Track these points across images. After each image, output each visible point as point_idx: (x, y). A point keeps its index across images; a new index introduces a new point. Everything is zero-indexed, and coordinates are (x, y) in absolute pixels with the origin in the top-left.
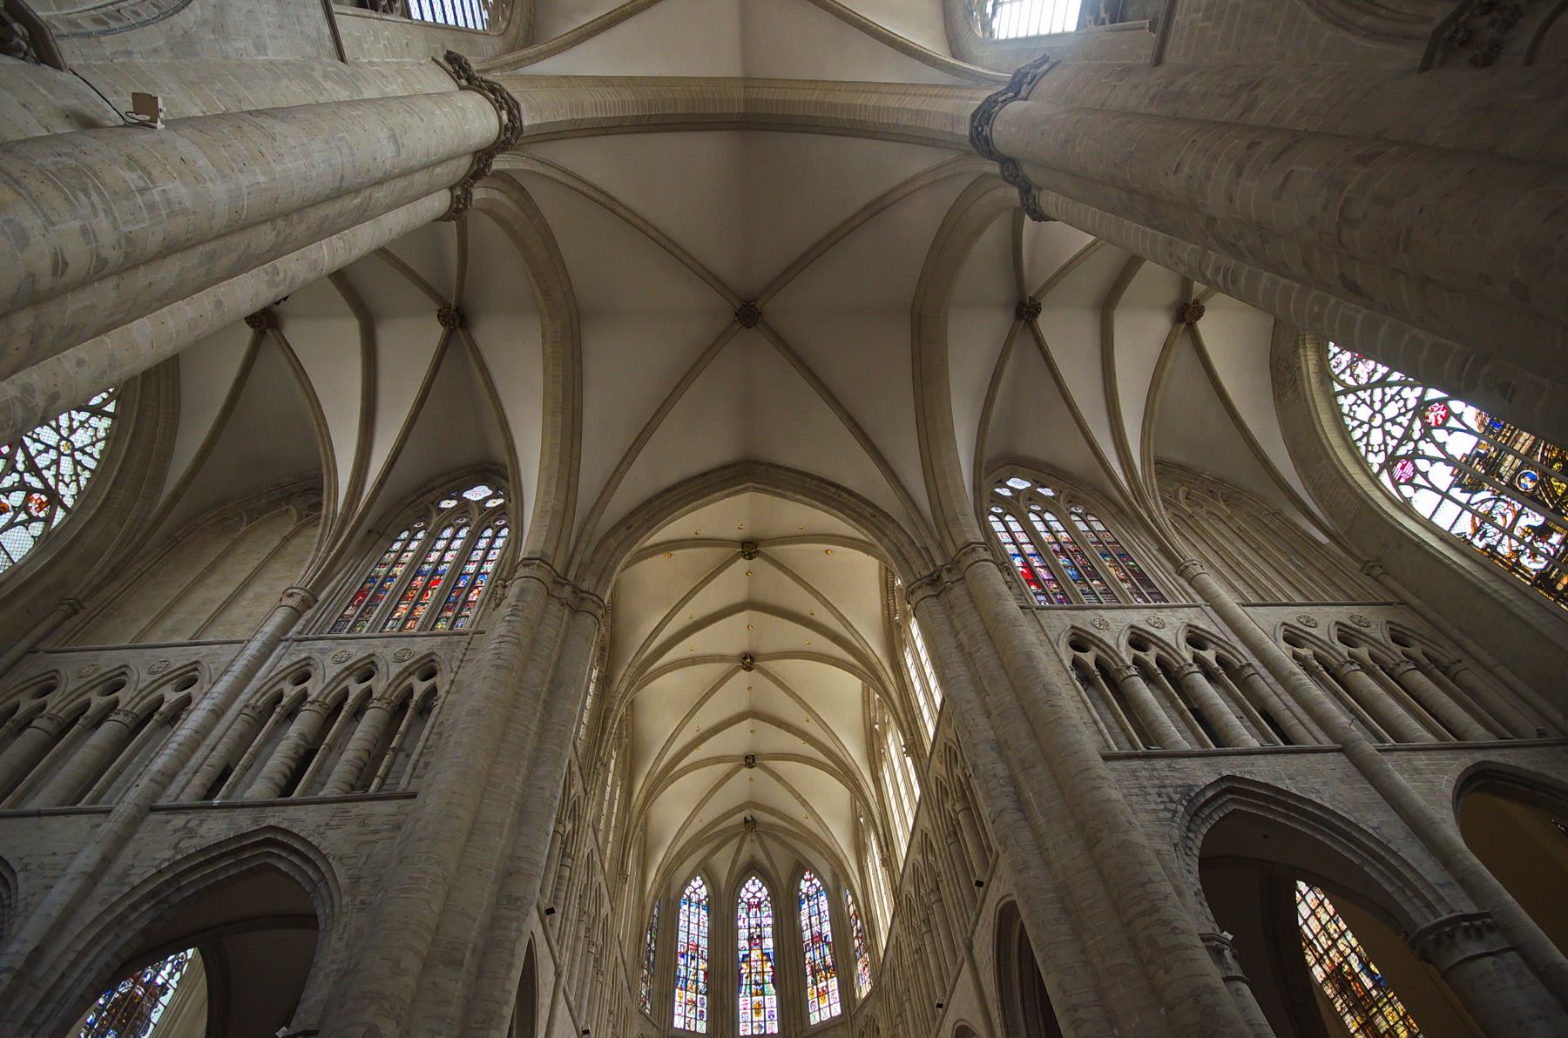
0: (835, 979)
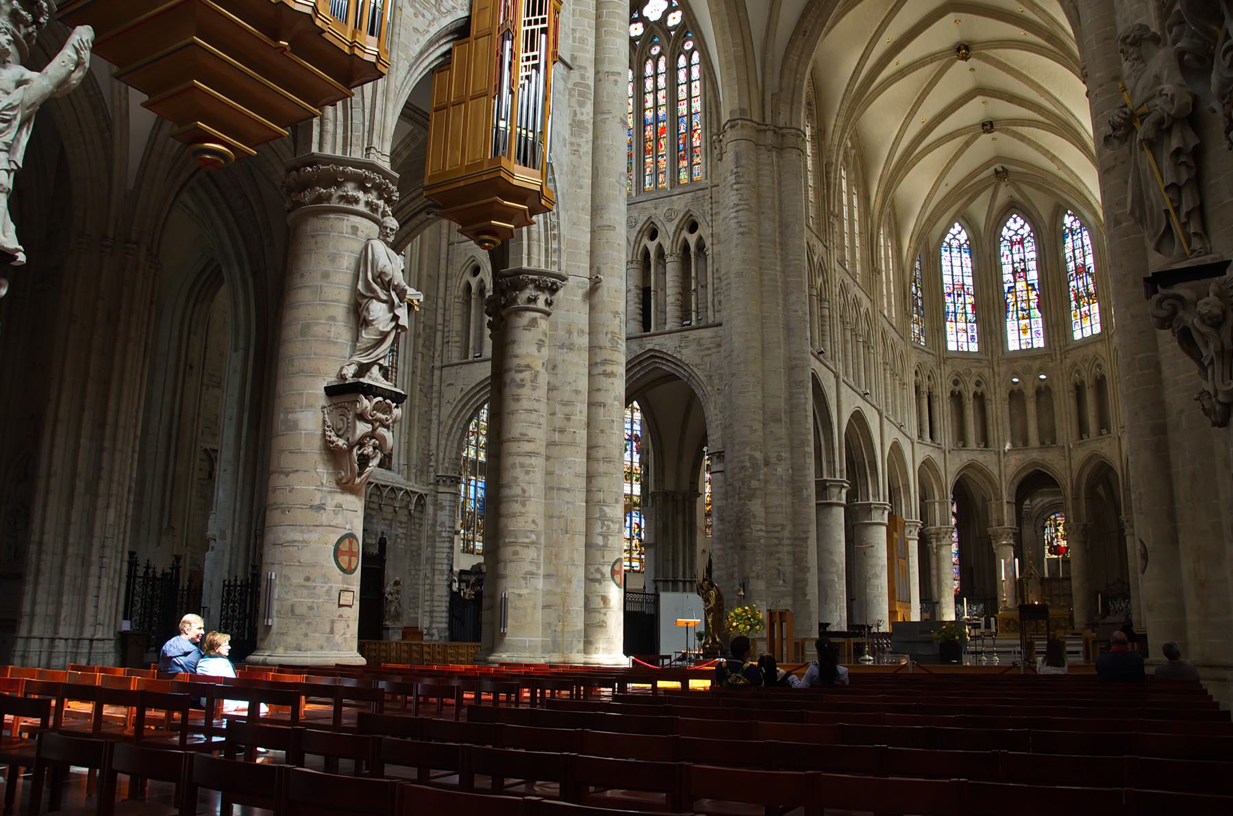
0: (1097, 304)
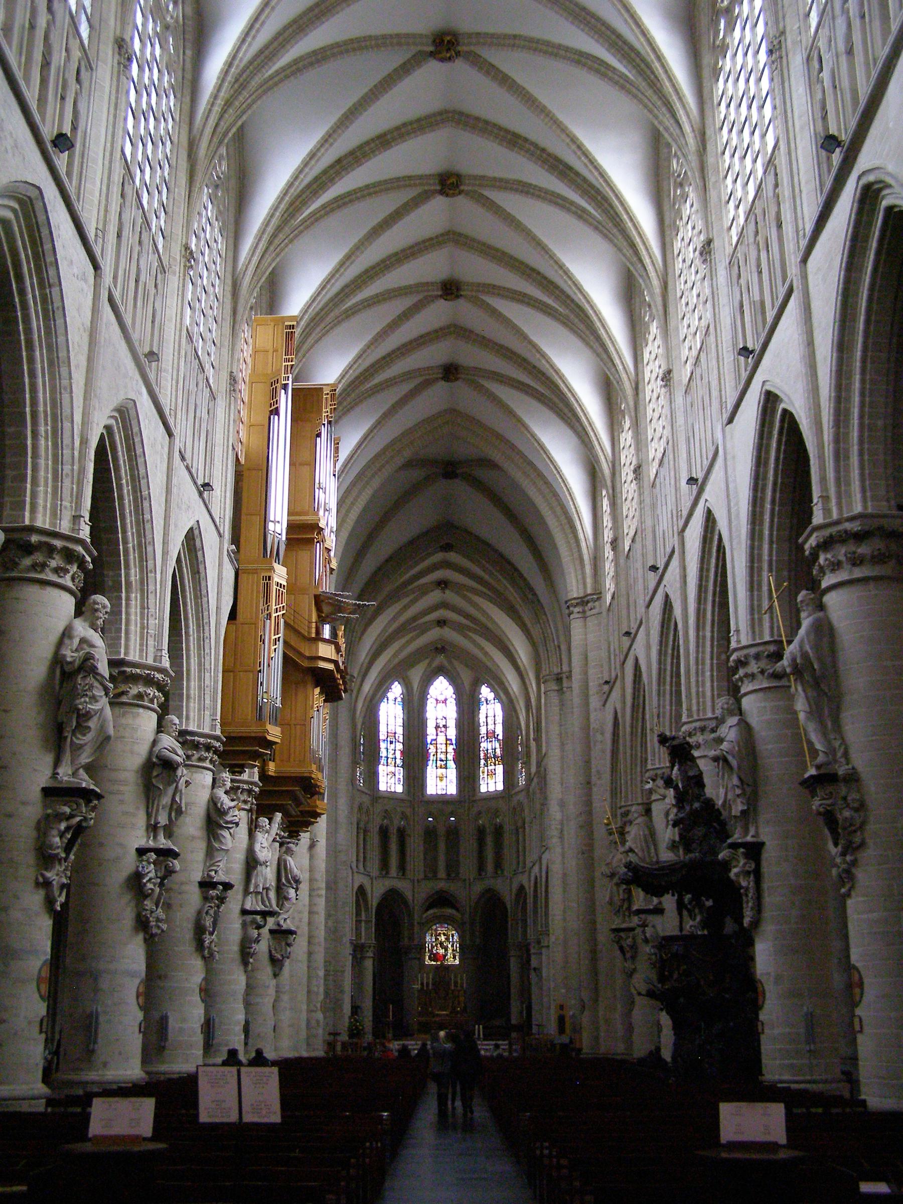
0: (501, 766)
